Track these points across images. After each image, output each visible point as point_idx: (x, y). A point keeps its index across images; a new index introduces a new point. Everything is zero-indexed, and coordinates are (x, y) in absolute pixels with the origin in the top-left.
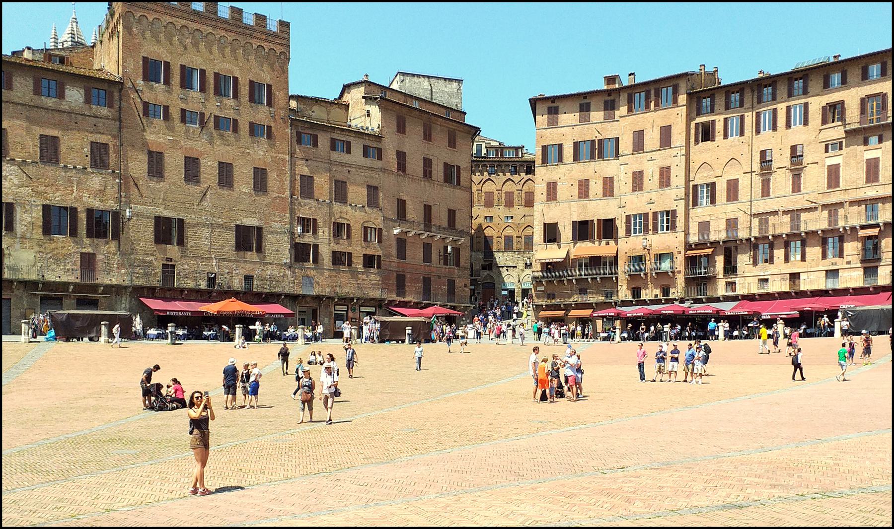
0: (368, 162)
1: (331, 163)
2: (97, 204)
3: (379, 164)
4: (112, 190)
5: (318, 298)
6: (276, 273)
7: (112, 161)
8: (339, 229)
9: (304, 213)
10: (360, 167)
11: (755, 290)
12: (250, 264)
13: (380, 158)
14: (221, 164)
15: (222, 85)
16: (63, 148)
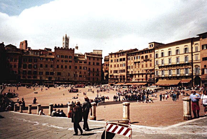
0: (85, 64)
1: (79, 64)
2: (51, 71)
3: (86, 64)
4: (53, 70)
5: (77, 81)
6: (72, 78)
7: (53, 66)
8: (80, 73)
9: (76, 71)
10: (83, 65)
11: (134, 81)
12: (69, 77)
13: (86, 63)
14: (65, 66)
15: (66, 57)
16: (48, 66)
